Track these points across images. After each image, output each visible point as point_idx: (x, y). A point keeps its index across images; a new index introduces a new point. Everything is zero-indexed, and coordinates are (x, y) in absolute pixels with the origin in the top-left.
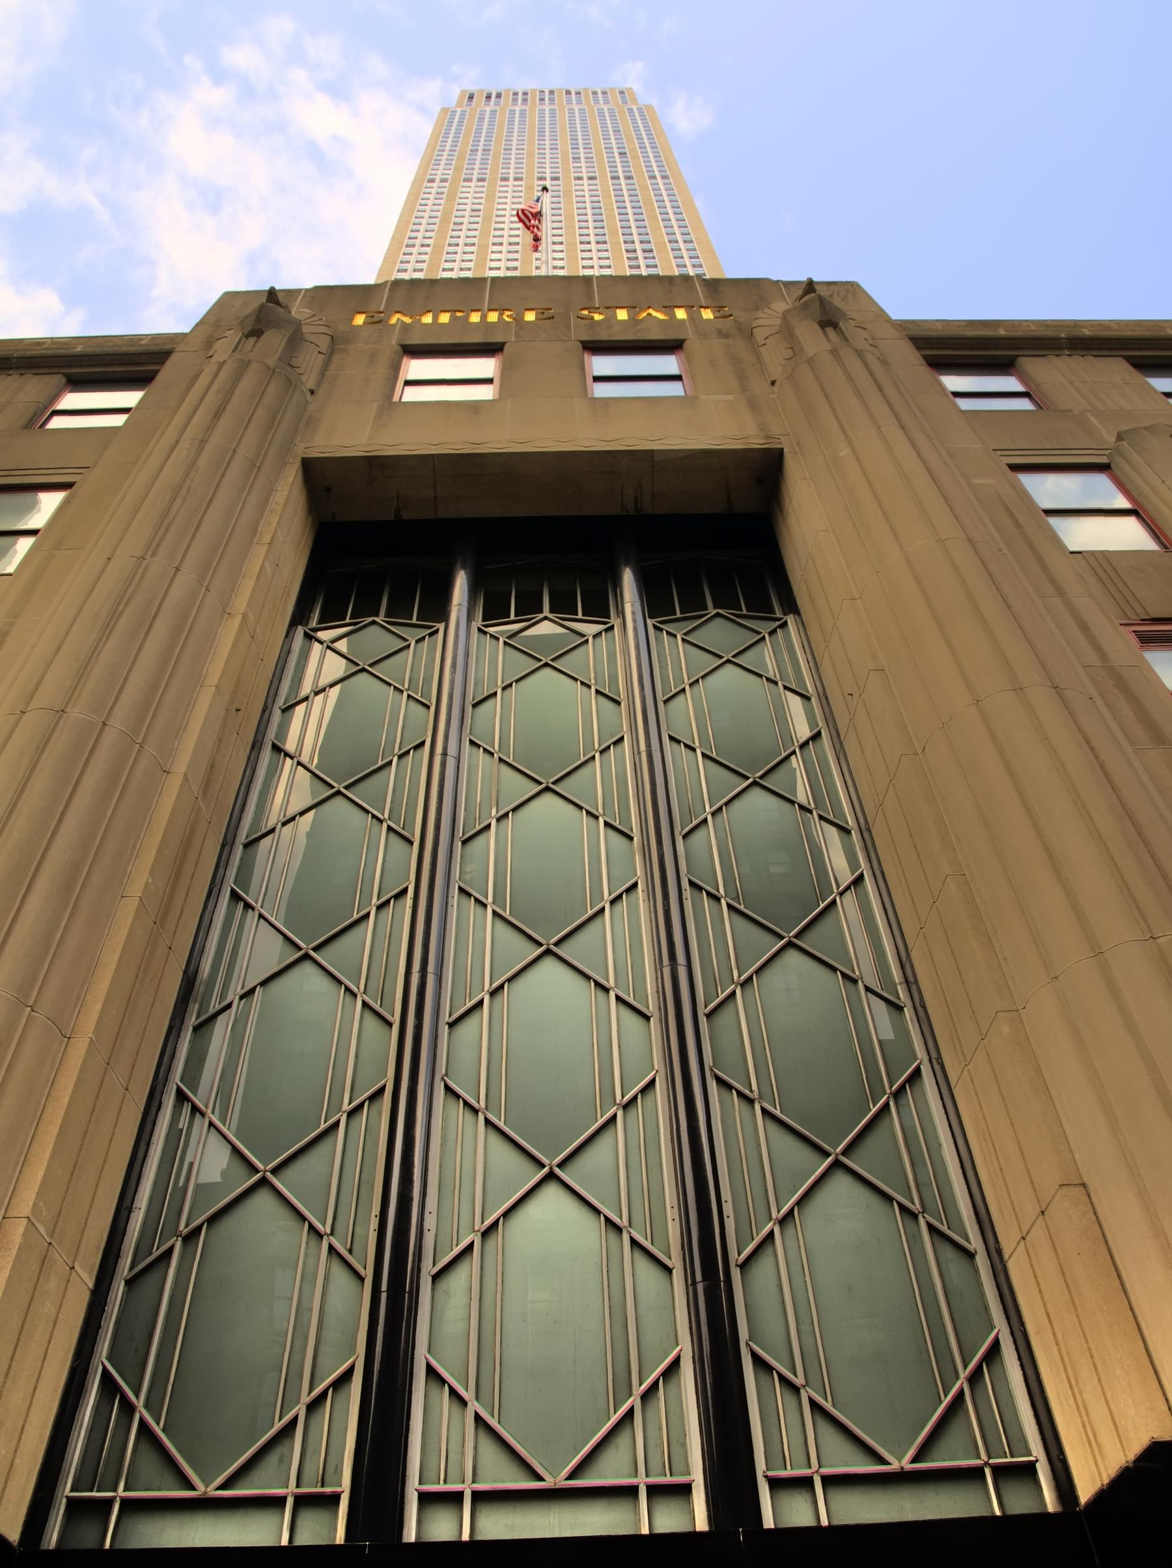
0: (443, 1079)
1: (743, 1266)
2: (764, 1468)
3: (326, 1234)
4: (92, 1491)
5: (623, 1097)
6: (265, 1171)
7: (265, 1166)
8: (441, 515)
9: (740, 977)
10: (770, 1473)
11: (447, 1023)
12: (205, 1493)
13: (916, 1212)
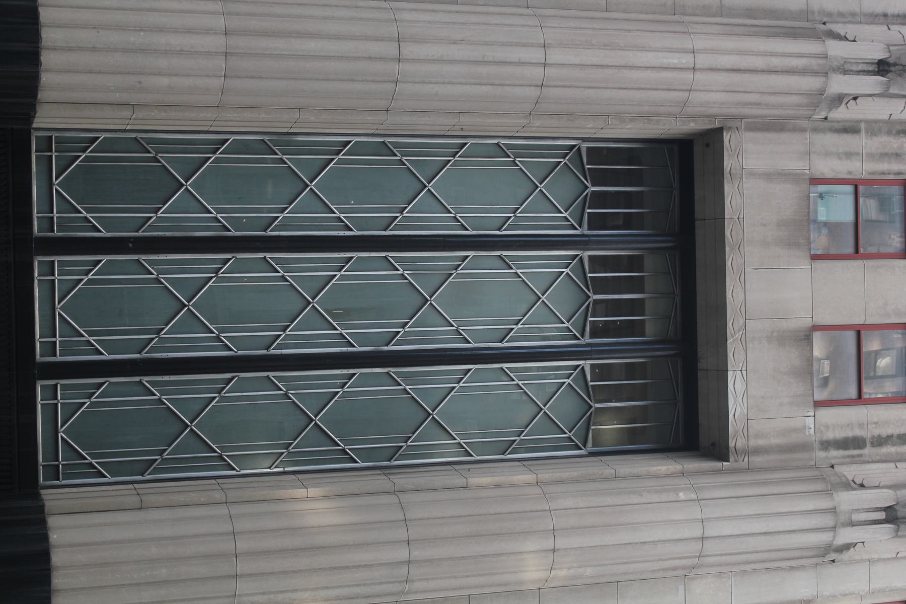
0: (233, 257)
1: (140, 382)
2: (61, 383)
3: (157, 215)
4: (55, 143)
5: (223, 337)
6: (186, 185)
7: (189, 185)
8: (697, 223)
9: (291, 394)
10: (59, 385)
11: (265, 257)
12: (54, 184)
13: (163, 455)
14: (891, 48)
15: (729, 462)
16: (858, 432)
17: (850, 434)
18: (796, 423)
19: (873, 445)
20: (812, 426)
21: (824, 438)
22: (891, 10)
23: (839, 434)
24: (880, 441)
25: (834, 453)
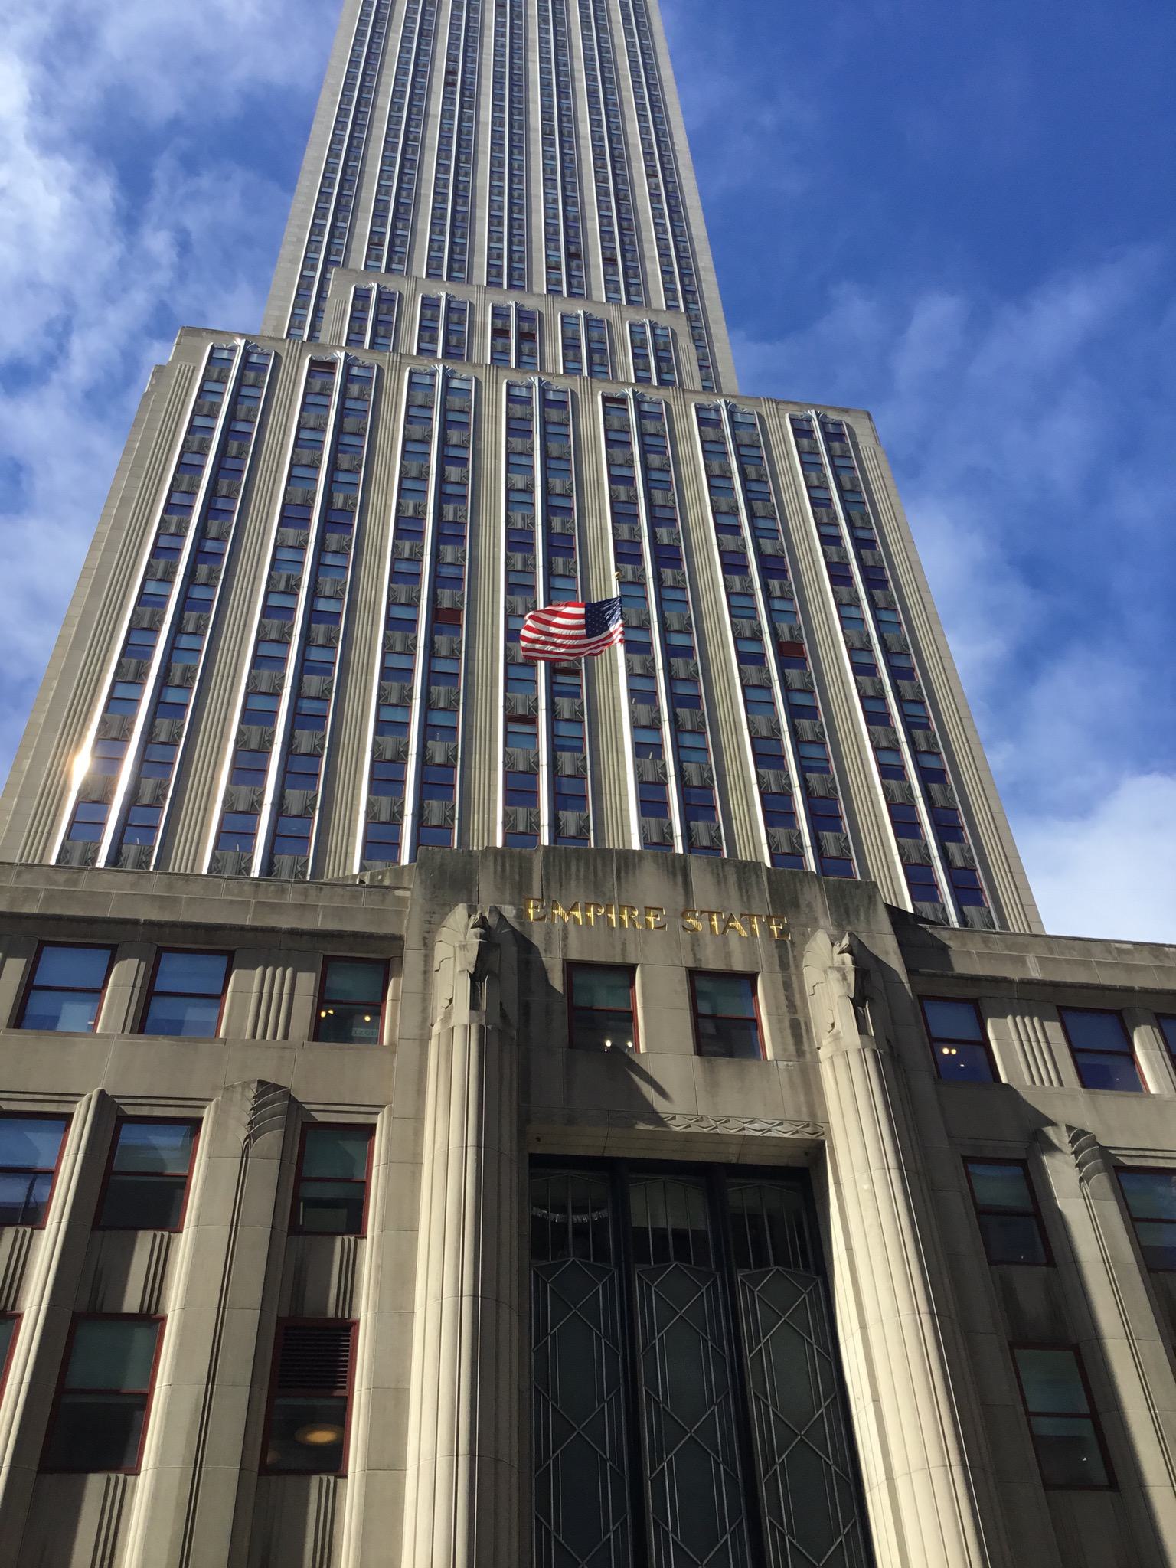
14: (458, 968)
15: (824, 1142)
16: (787, 1024)
17: (788, 1032)
18: (784, 1077)
19: (796, 1012)
20: (786, 1063)
21: (794, 1053)
22: (422, 968)
23: (790, 1040)
24: (792, 1006)
25: (806, 1047)
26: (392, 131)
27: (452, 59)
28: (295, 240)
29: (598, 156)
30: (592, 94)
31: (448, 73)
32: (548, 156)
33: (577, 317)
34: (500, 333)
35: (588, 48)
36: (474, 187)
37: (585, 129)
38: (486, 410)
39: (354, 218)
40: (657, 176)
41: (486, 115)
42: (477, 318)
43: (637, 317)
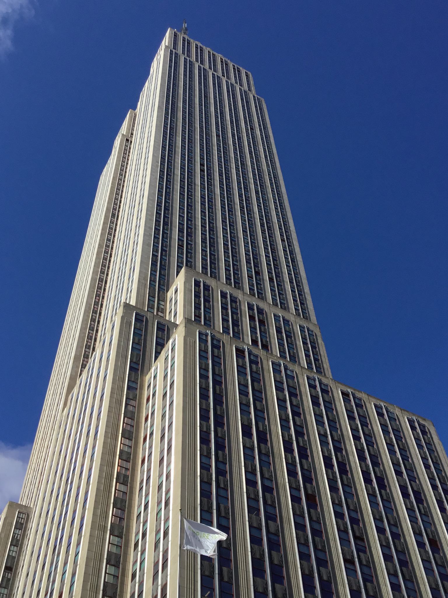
26: (182, 187)
27: (202, 158)
28: (148, 234)
29: (262, 225)
30: (257, 192)
31: (201, 164)
32: (243, 220)
33: (279, 317)
34: (252, 318)
35: (253, 169)
36: (216, 227)
37: (256, 209)
38: (302, 389)
39: (171, 229)
40: (285, 241)
41: (218, 191)
42: (242, 308)
43: (301, 323)
